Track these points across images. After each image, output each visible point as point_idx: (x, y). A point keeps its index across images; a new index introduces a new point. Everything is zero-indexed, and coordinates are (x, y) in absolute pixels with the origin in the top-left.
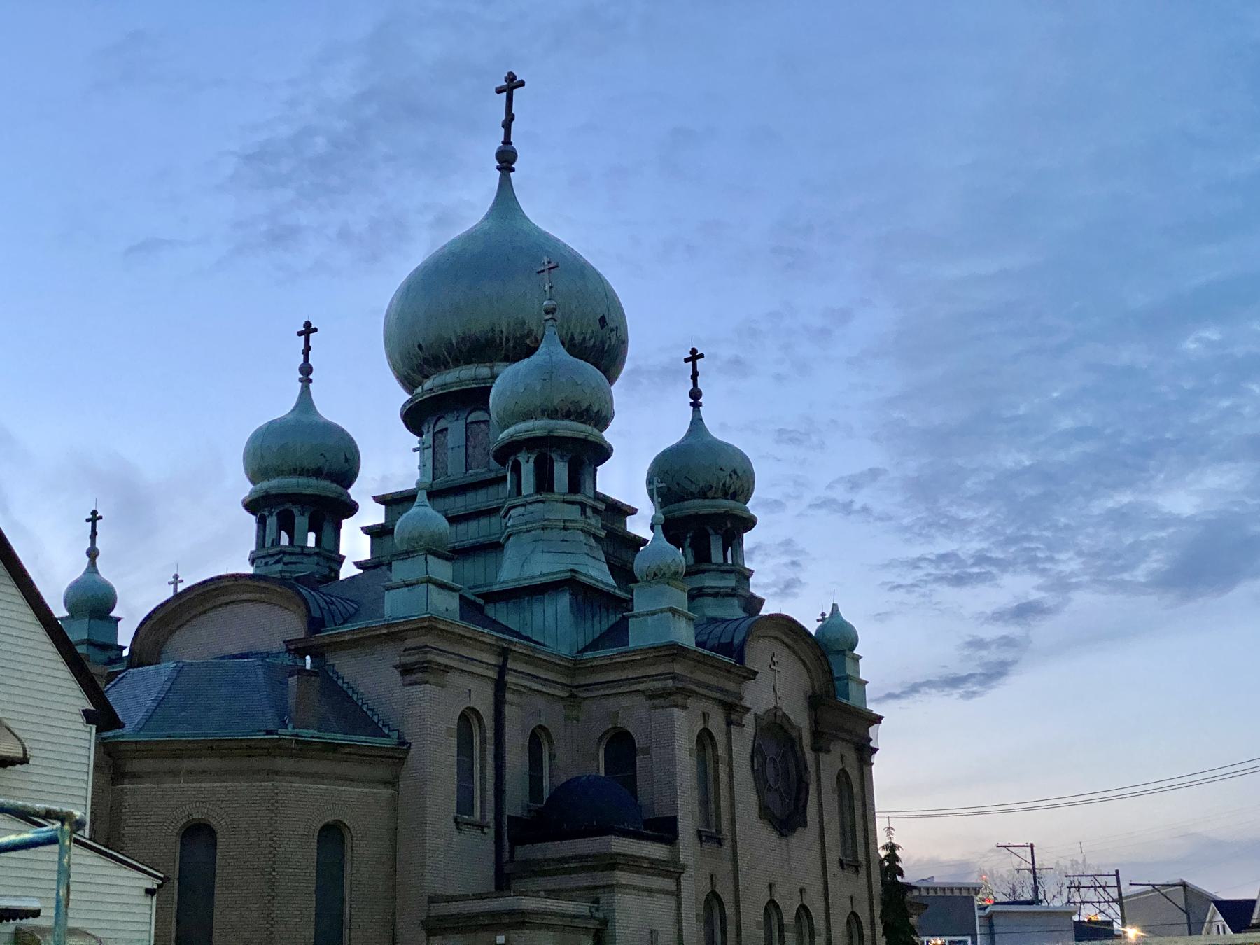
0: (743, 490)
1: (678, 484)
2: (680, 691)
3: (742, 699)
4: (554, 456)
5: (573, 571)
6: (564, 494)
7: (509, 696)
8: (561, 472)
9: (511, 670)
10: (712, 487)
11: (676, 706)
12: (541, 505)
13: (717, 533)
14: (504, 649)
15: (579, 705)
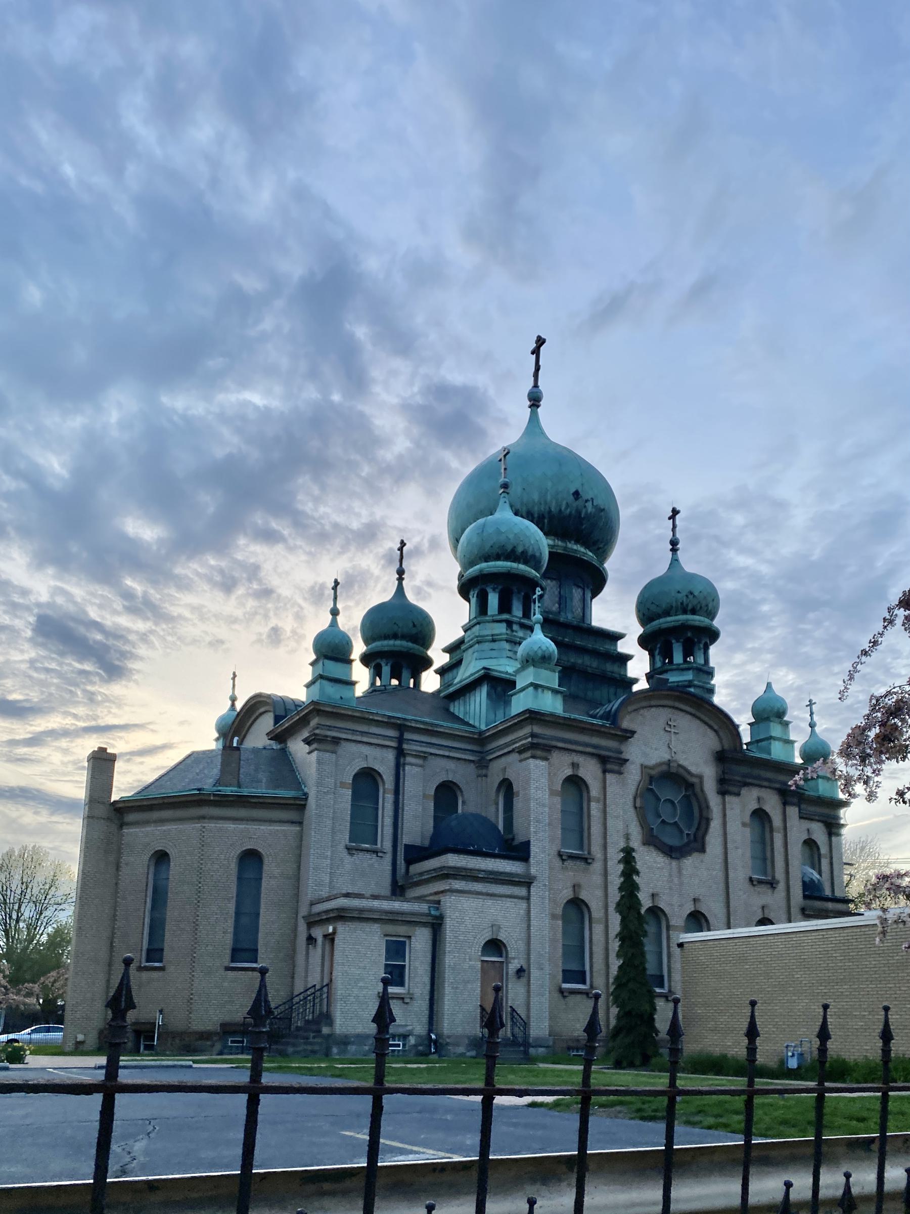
0: (701, 607)
1: (648, 609)
2: (533, 746)
3: (621, 753)
4: (489, 590)
5: (484, 668)
6: (520, 618)
7: (409, 759)
8: (493, 600)
9: (406, 739)
10: (672, 607)
11: (533, 757)
12: (478, 626)
13: (678, 641)
14: (400, 725)
15: (487, 767)
